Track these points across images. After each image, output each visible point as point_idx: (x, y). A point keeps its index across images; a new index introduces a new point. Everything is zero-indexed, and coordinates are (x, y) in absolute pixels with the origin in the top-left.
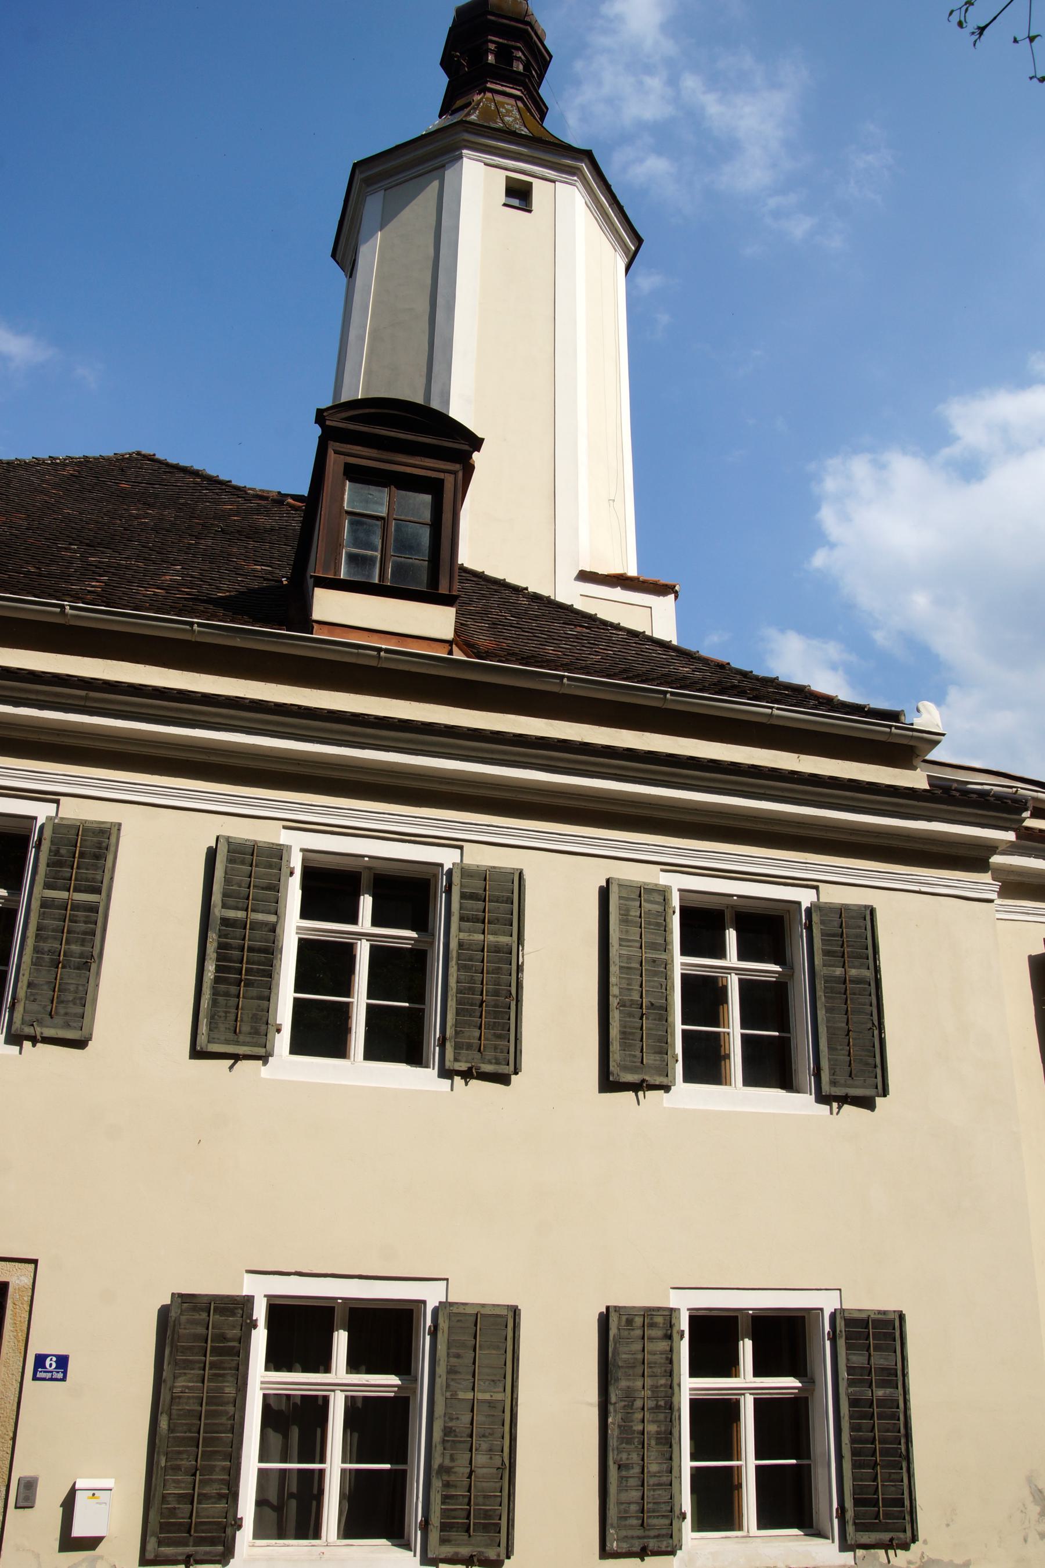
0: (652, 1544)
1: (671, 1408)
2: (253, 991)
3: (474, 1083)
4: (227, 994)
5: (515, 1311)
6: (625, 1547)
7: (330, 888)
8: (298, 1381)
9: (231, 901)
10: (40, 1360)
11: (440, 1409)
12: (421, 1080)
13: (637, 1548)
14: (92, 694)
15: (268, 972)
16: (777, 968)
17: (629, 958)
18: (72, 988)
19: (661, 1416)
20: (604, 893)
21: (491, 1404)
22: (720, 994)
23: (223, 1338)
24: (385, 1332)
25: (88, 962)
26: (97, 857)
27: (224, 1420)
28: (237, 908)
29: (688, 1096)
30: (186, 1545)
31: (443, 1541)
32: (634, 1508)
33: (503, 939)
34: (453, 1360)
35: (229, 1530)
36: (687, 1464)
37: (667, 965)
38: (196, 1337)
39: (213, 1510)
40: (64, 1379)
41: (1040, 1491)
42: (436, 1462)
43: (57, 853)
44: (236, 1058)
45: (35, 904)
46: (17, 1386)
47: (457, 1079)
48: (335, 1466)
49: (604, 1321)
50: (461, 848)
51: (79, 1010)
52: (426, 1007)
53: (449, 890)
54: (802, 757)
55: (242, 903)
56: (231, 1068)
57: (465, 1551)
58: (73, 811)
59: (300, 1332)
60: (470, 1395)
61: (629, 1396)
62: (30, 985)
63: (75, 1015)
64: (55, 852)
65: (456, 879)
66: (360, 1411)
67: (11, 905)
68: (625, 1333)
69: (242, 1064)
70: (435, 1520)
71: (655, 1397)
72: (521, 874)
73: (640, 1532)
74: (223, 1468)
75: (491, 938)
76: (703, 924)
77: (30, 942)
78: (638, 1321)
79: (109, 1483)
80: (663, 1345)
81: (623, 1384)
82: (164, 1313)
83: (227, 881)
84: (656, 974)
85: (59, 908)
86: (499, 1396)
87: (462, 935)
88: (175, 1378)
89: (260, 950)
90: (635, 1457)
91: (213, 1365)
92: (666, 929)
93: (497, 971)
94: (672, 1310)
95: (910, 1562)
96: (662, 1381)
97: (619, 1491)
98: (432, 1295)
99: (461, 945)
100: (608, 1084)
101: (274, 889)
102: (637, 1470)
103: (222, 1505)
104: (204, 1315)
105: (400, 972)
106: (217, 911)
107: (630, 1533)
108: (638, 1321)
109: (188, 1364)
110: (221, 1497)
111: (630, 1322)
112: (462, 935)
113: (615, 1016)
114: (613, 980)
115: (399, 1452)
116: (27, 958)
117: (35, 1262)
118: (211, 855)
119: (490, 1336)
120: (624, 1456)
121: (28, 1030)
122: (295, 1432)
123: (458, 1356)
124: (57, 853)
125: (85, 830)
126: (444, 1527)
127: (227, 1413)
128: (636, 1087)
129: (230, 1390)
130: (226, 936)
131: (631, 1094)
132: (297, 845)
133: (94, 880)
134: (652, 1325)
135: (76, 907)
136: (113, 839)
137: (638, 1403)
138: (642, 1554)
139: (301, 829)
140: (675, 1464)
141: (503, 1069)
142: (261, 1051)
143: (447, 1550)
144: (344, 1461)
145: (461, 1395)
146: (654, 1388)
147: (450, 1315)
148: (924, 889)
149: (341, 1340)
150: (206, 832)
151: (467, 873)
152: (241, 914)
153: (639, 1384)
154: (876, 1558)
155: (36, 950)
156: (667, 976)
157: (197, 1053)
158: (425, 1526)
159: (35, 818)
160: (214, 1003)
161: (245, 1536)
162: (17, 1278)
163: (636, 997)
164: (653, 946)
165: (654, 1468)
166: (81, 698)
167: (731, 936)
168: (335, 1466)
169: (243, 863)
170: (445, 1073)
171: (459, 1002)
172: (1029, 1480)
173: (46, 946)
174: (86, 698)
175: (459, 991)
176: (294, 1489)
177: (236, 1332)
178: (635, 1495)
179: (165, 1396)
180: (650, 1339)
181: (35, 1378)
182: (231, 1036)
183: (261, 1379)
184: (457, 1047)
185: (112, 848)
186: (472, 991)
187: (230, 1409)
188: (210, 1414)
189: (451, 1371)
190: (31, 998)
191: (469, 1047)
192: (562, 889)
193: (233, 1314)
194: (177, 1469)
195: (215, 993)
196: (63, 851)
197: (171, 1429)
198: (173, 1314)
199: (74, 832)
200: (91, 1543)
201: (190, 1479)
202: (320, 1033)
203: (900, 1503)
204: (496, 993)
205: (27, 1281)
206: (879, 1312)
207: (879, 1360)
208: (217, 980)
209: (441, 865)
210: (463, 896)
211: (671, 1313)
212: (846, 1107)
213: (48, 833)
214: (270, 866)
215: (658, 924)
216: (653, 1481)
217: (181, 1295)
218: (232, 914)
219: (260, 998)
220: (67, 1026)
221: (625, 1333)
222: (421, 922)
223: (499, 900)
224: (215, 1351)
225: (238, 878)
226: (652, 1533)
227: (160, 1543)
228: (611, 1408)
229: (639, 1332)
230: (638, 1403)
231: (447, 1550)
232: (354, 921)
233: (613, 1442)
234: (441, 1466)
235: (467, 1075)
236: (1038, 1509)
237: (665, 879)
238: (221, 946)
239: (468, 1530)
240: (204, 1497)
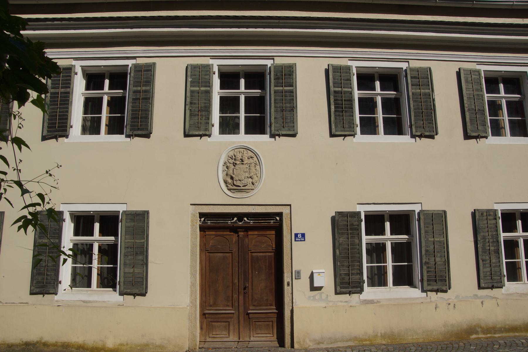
0: (495, 285)
1: (498, 242)
2: (348, 114)
3: (422, 139)
4: (339, 116)
5: (445, 212)
6: (486, 286)
7: (366, 79)
8: (375, 238)
9: (336, 85)
10: (296, 235)
11: (423, 244)
12: (405, 139)
13: (490, 286)
14: (281, 21)
15: (352, 108)
16: (519, 96)
17: (470, 94)
18: (289, 118)
19: (495, 244)
20: (458, 74)
21: (440, 242)
22: (500, 107)
23: (352, 225)
24: (401, 221)
25: (293, 109)
26: (290, 75)
27: (356, 250)
28: (338, 87)
29: (492, 140)
30: (349, 288)
31: (428, 285)
32: (488, 273)
33: (427, 91)
34: (426, 228)
35: (361, 283)
36: (504, 261)
37: (482, 96)
38: (344, 225)
39: (356, 277)
40: (304, 240)
42: (424, 261)
43: (276, 75)
44: (345, 136)
45: (272, 92)
46: (290, 243)
47: (417, 138)
48: (390, 264)
49: (474, 214)
50: (408, 62)
51: (293, 125)
52: (402, 116)
53: (406, 76)
54: (525, 19)
55: (340, 85)
56: (344, 139)
57: (435, 288)
58: (279, 61)
59: (375, 222)
60: (433, 239)
61: (484, 238)
62: (275, 118)
63: (291, 126)
64: (276, 75)
65: (408, 72)
66: (396, 247)
67: (263, 95)
68: (481, 218)
69: (347, 138)
70: (425, 278)
71: (492, 238)
72: (430, 69)
73: (491, 281)
74: (357, 265)
75: (423, 91)
76: (492, 82)
77: (273, 104)
78: (485, 214)
79: (323, 271)
80: (494, 221)
81: (482, 234)
82: (333, 219)
83: (334, 79)
84: (479, 99)
85: (280, 93)
86: (442, 239)
87: (413, 91)
88: (339, 238)
89: (348, 100)
90: (488, 258)
91: (351, 234)
92: (481, 84)
93: (426, 101)
94: (495, 210)
96: (494, 233)
97: (483, 268)
98: (417, 208)
99: (413, 94)
100: (467, 136)
101: (349, 80)
102: (488, 261)
103: (358, 276)
104: (346, 218)
105: (392, 106)
106: (332, 89)
107: (488, 281)
108: (485, 214)
109: (343, 234)
110: (357, 274)
111: (482, 214)
112: (413, 91)
113: (467, 114)
114: (465, 102)
115: (409, 259)
116: (273, 110)
117: (290, 205)
118: (327, 72)
119: (437, 220)
120: (484, 257)
121: (277, 133)
122: (375, 255)
123: (428, 227)
124: (276, 75)
125: (285, 67)
126: (428, 280)
127: (356, 248)
128: (476, 137)
129: (357, 241)
130: (336, 97)
131: (475, 140)
132: (354, 65)
133: (290, 82)
134: (490, 215)
135: (286, 92)
136: (294, 69)
137: (487, 240)
138: (492, 287)
139: (356, 60)
140: (501, 259)
141: (432, 134)
142: (353, 133)
143: (430, 288)
144: (392, 263)
145: (430, 239)
146: (492, 235)
147: (424, 214)
149: (388, 225)
150: (324, 64)
151: (412, 70)
152: (340, 89)
153: (487, 234)
155: (275, 107)
156: (483, 100)
157: (332, 135)
158: (422, 280)
159: (267, 65)
160: (336, 119)
161: (365, 285)
162: (285, 211)
163: (473, 107)
164: (477, 90)
165: (494, 261)
166: (277, 23)
167: (501, 86)
168: (390, 264)
169: (338, 72)
170: (413, 136)
171: (415, 113)
173: (278, 105)
174: (279, 23)
175: (414, 109)
176: (376, 273)
177: (356, 223)
178: (489, 269)
179: (337, 244)
180: (490, 220)
181: (295, 241)
182: (343, 129)
183: (365, 239)
184: (416, 127)
185: (294, 72)
186: (419, 109)
187: (358, 247)
188: (352, 249)
189: (426, 232)
190: (276, 122)
191: (420, 127)
192: (444, 72)
193: (355, 217)
194: (343, 266)
195: (335, 115)
196: (278, 74)
197: (340, 254)
198: (337, 218)
199: (281, 68)
200: (320, 288)
201: (347, 269)
202: (369, 127)
204: (427, 109)
205: (289, 211)
208: (335, 111)
209: (402, 68)
210: (411, 77)
211: (495, 211)
213: (272, 69)
214: (347, 73)
215: (478, 82)
216: (494, 265)
217: (338, 212)
218: (337, 89)
219: (351, 116)
220: (290, 130)
221: (481, 218)
222: (396, 88)
223: (424, 78)
224: (351, 229)
225: (336, 78)
226: (495, 281)
227: (341, 288)
228: (479, 242)
229: (485, 217)
230: (487, 240)
231: (430, 288)
232: (374, 90)
233: (480, 253)
234: (425, 262)
235: (420, 136)
237: (478, 67)
238: (335, 100)
239: (436, 281)
240: (352, 274)
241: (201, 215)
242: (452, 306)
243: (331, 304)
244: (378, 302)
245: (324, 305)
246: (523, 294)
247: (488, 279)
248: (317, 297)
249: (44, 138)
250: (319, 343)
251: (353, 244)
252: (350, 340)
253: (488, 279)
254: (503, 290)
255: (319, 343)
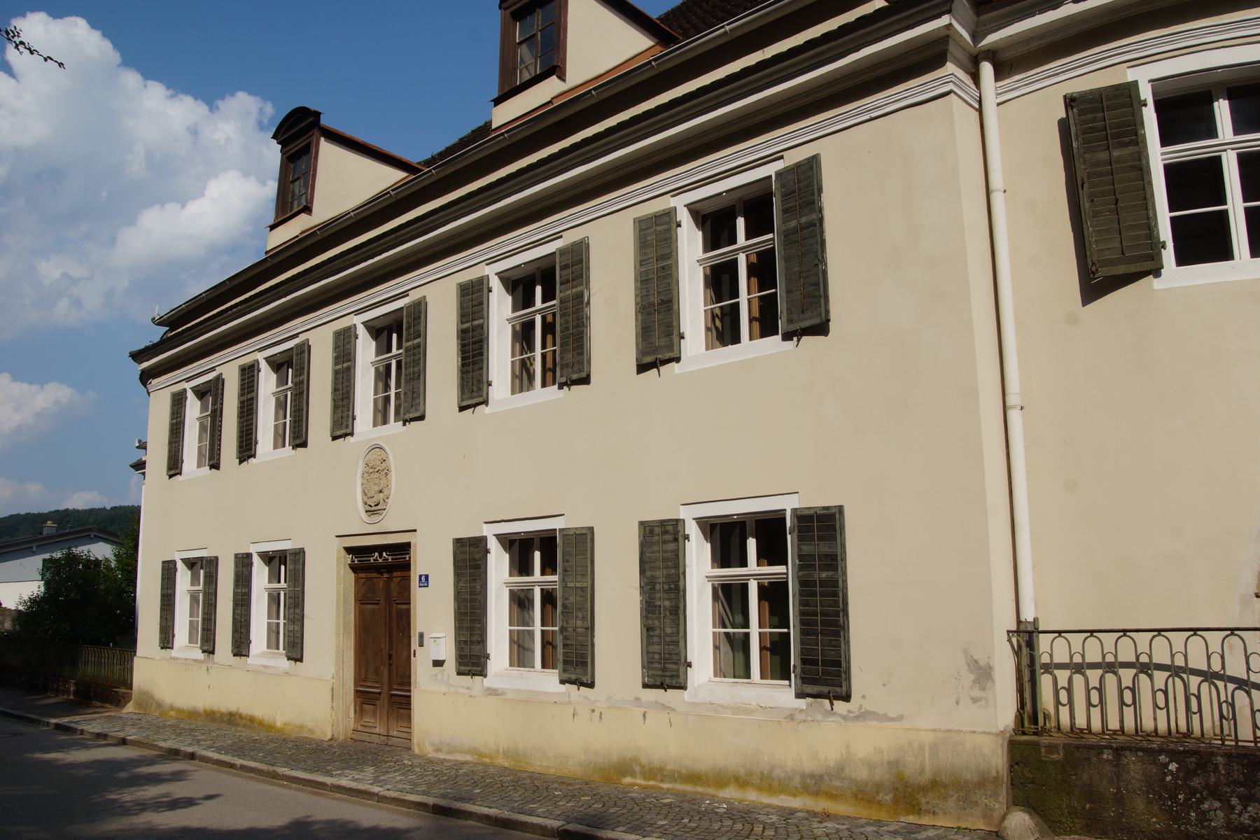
3: (573, 387)
13: (658, 683)
41: (976, 662)
57: (573, 677)
73: (660, 673)
78: (657, 530)
94: (677, 520)
95: (850, 712)
107: (656, 672)
138: (662, 686)
148: (873, 115)
154: (822, 705)
172: (966, 652)
175: (562, 332)
203: (837, 663)
206: (824, 508)
207: (824, 548)
212: (804, 338)
226: (669, 674)
236: (972, 677)
241: (349, 550)
242: (597, 714)
243: (452, 690)
244: (503, 694)
245: (444, 689)
246: (721, 706)
247: (656, 669)
248: (439, 677)
249: (241, 462)
250: (438, 750)
251: (473, 593)
252: (469, 752)
253: (656, 669)
254: (685, 695)
255: (438, 750)
